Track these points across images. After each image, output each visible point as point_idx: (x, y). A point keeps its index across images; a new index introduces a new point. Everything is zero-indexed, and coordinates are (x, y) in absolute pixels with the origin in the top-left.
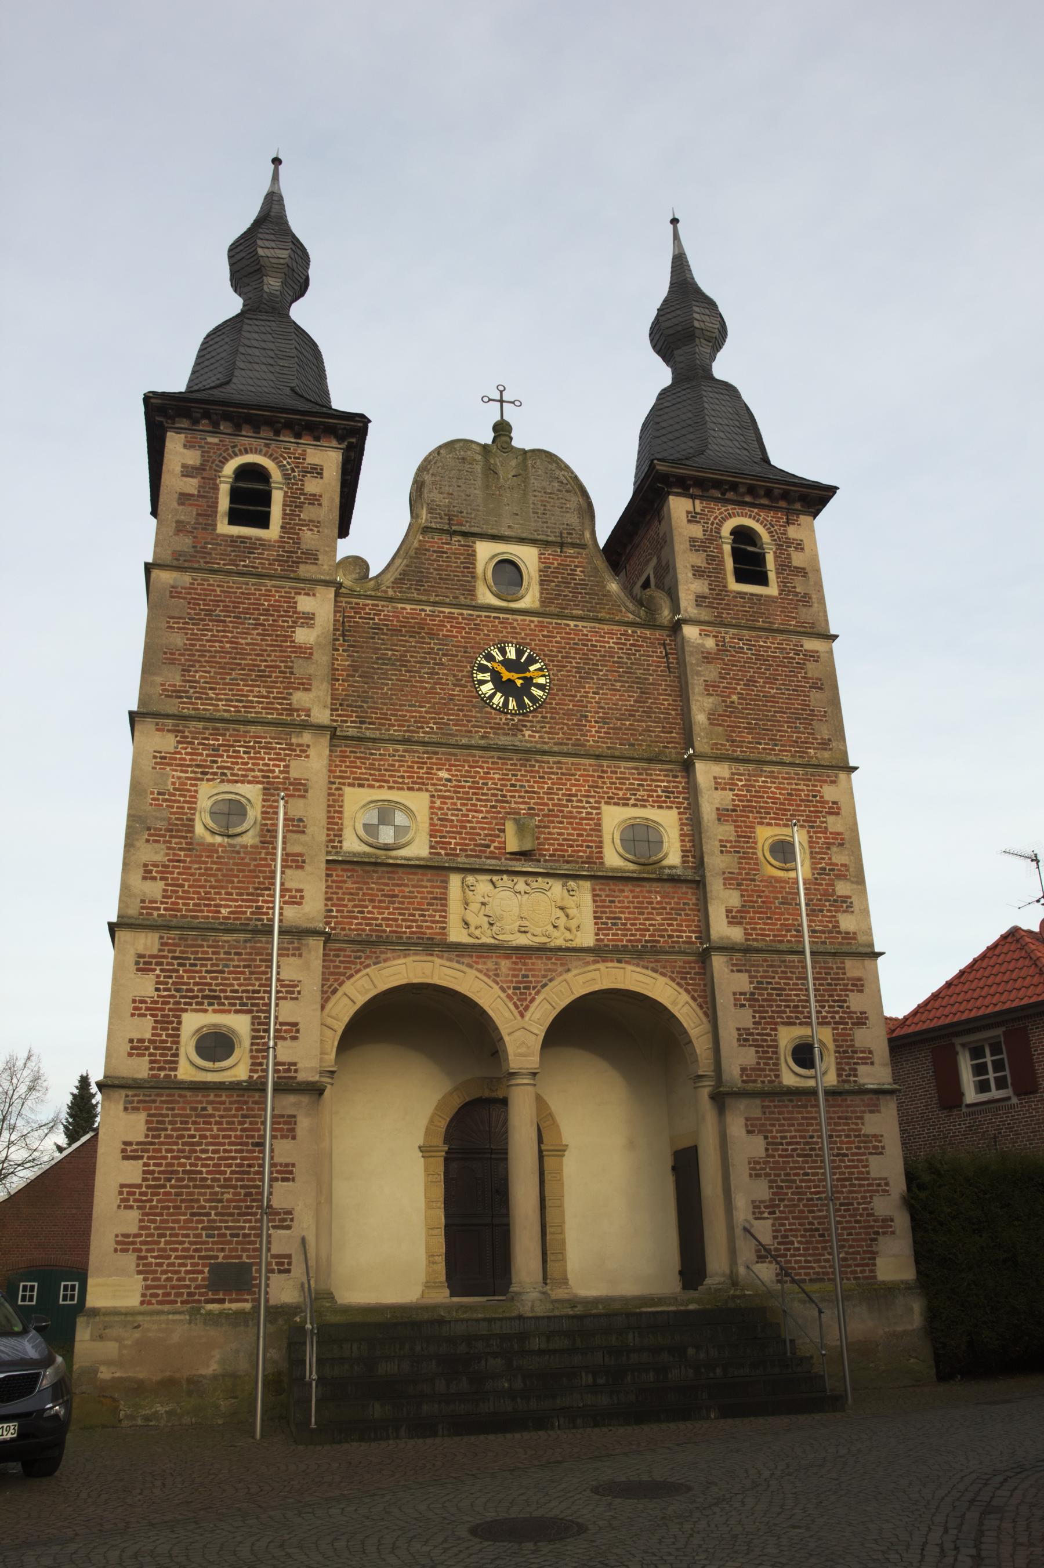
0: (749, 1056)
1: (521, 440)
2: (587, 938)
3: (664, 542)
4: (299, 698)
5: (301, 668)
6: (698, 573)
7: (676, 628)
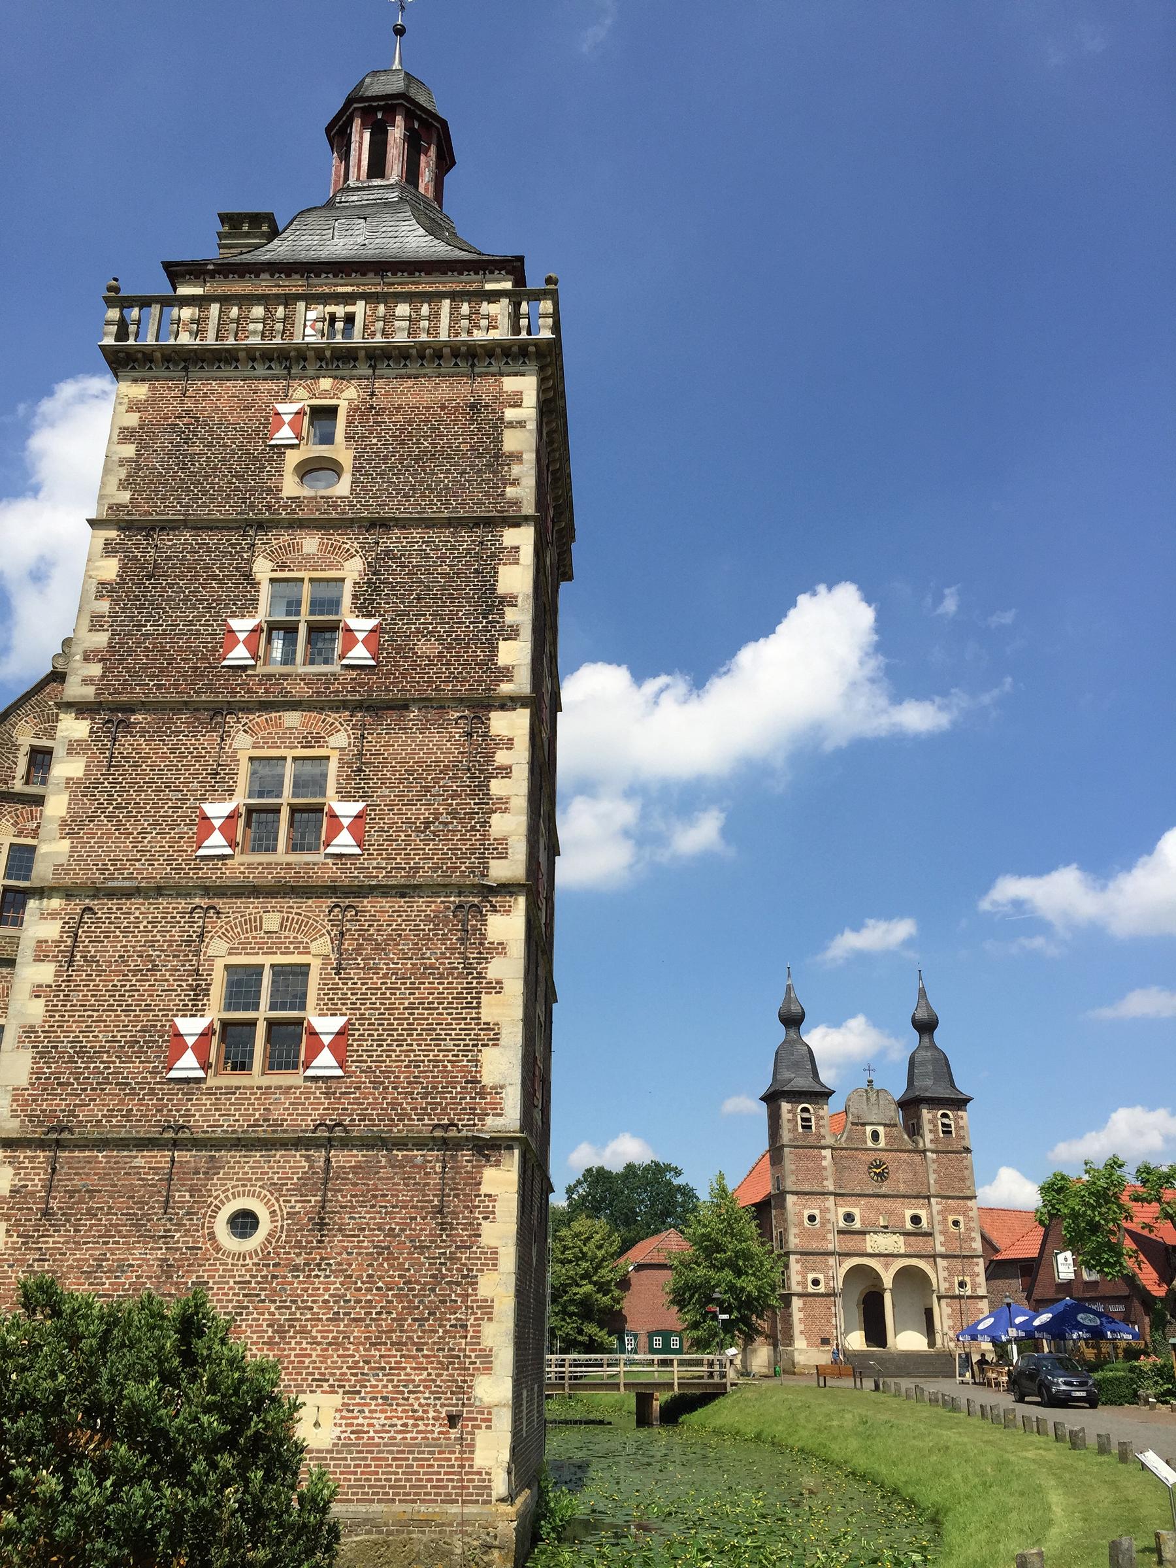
0: (947, 1285)
1: (876, 1086)
2: (902, 1251)
3: (919, 1117)
4: (825, 1183)
5: (825, 1173)
6: (931, 1131)
7: (924, 1151)
